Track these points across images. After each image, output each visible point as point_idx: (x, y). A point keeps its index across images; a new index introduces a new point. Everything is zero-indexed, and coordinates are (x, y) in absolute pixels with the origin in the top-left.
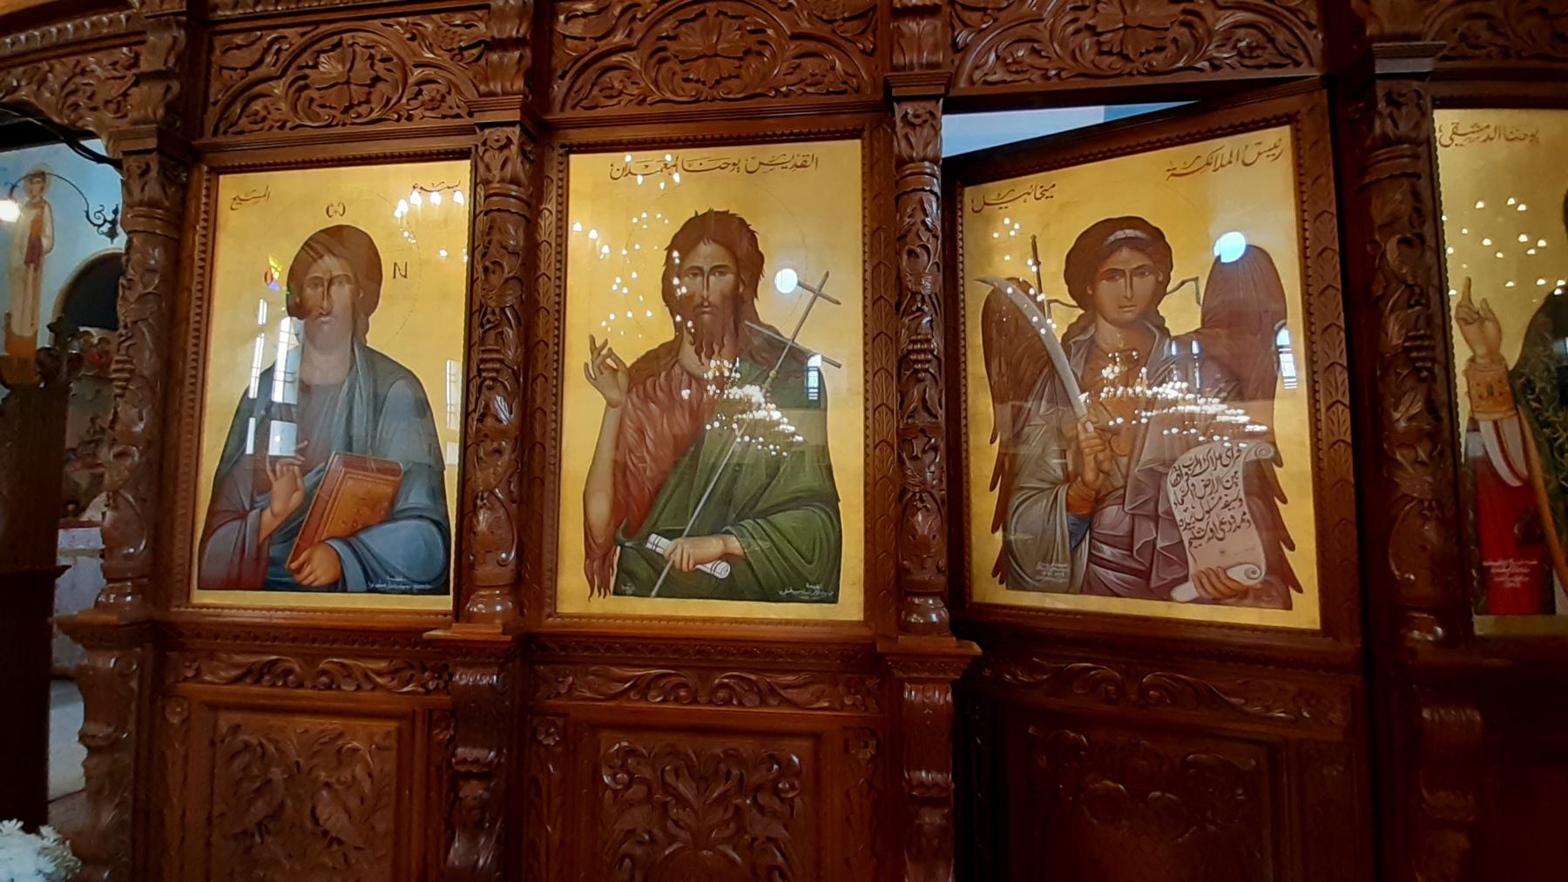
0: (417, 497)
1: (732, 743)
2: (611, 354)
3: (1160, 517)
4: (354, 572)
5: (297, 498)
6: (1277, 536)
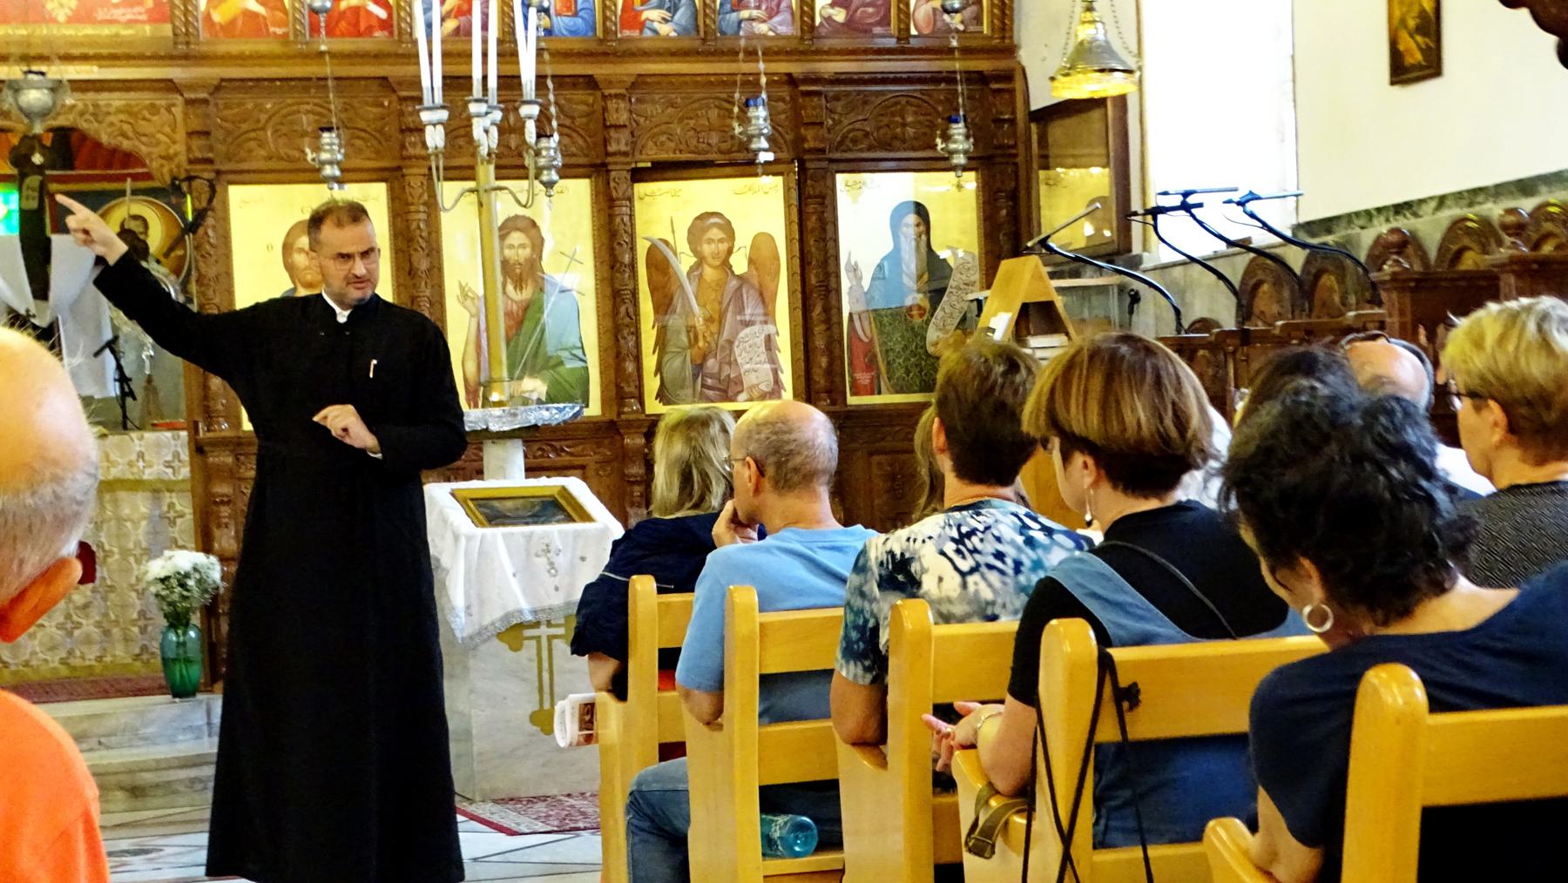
2: (470, 290)
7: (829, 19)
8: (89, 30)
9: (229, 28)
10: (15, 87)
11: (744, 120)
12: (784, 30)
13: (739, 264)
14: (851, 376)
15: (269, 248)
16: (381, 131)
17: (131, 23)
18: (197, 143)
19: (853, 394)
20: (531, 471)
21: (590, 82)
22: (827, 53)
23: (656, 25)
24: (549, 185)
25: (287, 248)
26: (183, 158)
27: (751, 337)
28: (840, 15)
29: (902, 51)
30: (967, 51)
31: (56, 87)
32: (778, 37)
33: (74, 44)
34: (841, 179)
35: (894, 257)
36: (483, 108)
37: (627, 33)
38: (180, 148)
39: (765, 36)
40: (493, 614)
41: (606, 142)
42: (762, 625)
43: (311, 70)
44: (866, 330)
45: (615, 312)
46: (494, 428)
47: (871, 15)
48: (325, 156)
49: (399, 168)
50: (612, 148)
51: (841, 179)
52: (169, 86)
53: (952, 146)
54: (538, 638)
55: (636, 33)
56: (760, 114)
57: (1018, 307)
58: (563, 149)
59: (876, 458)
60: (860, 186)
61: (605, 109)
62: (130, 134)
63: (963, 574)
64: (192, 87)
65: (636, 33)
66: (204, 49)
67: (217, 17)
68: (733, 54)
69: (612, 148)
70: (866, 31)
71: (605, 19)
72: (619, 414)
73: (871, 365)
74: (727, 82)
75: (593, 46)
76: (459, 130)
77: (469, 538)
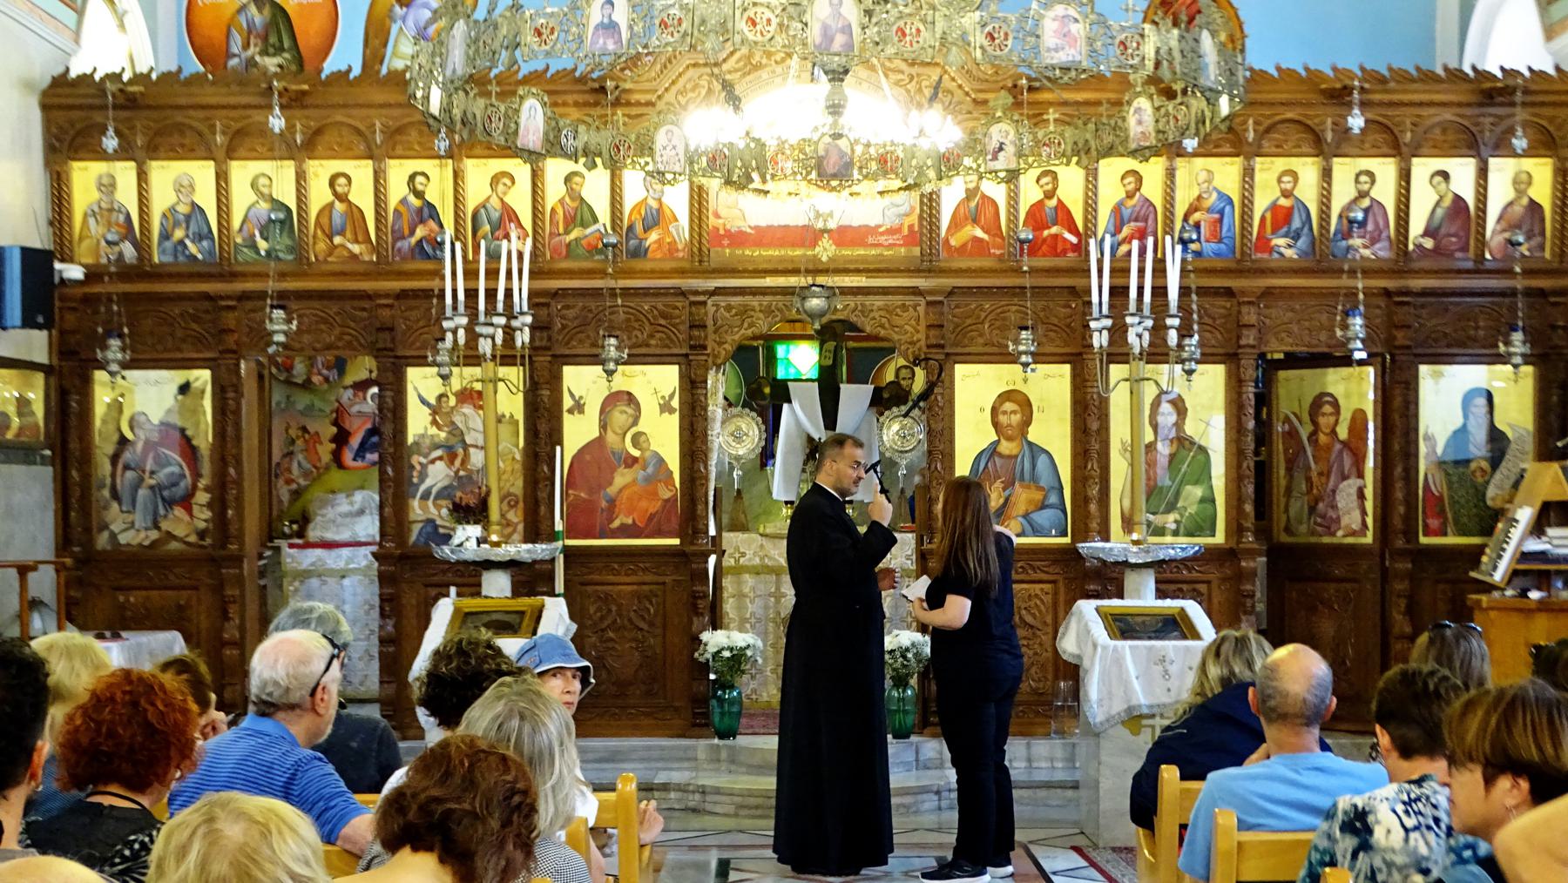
0: (1053, 499)
1: (1180, 586)
3: (1334, 507)
4: (1028, 528)
5: (1002, 501)
6: (1364, 513)
7: (1419, 246)
8: (862, 252)
9: (962, 250)
10: (803, 293)
11: (1345, 327)
12: (1382, 254)
13: (1343, 433)
14: (1424, 521)
15: (982, 410)
16: (1069, 326)
17: (891, 246)
18: (932, 332)
19: (1426, 534)
20: (1161, 594)
21: (1229, 293)
22: (1417, 272)
23: (1282, 250)
24: (1190, 372)
25: (995, 411)
26: (923, 343)
27: (1348, 489)
28: (1429, 243)
29: (1479, 270)
30: (1527, 273)
31: (831, 292)
32: (1378, 259)
33: (851, 261)
34: (1424, 369)
35: (1461, 434)
36: (1136, 320)
37: (1259, 255)
38: (922, 336)
39: (1368, 259)
40: (1118, 707)
41: (1239, 337)
42: (1239, 844)
43: (1017, 281)
44: (1439, 485)
45: (1239, 466)
46: (1132, 560)
47: (1454, 243)
48: (1022, 348)
49: (1080, 354)
50: (1243, 342)
51: (1424, 369)
52: (915, 291)
53: (1512, 350)
54: (1153, 727)
55: (1265, 256)
56: (1357, 323)
57: (1538, 505)
58: (1201, 344)
59: (1441, 587)
60: (1440, 375)
61: (1239, 312)
62: (887, 325)
63: (1406, 830)
64: (931, 292)
65: (1265, 256)
66: (942, 265)
67: (953, 242)
68: (1339, 272)
69: (1243, 342)
70: (1450, 255)
71: (1243, 244)
72: (1239, 542)
73: (1441, 514)
74: (1333, 294)
75: (1233, 265)
76: (1118, 331)
77: (1105, 648)
